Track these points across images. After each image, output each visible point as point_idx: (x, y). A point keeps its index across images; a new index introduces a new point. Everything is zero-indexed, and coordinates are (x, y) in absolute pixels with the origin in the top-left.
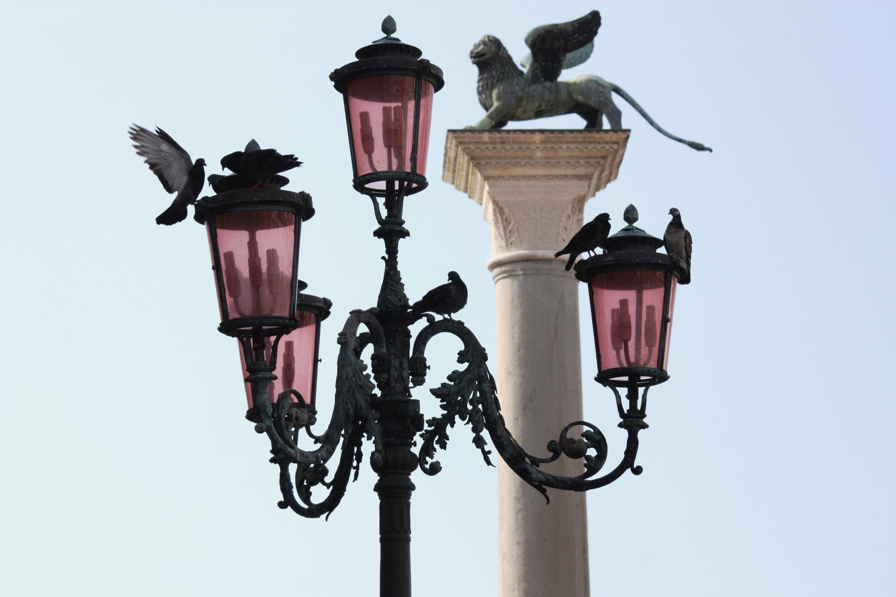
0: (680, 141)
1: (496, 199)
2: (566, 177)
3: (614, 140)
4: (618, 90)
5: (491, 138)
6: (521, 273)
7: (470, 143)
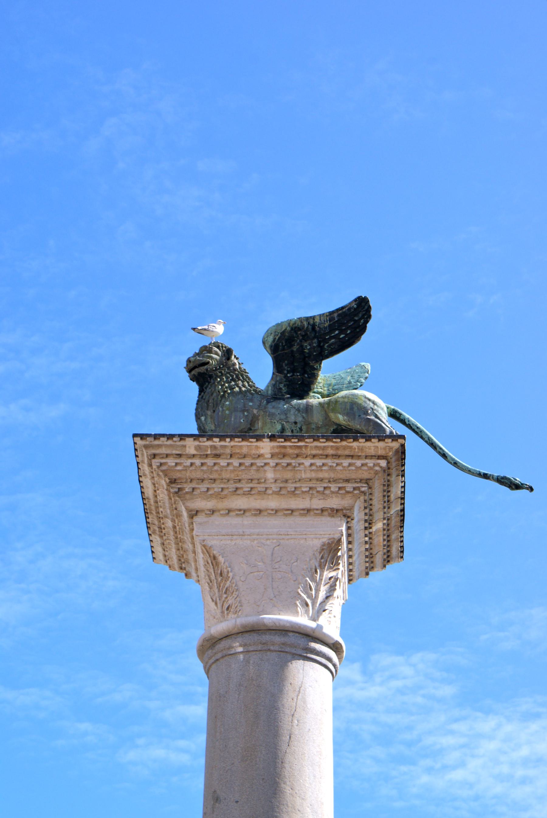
0: (485, 476)
1: (209, 543)
2: (308, 511)
3: (381, 452)
4: (394, 415)
5: (198, 448)
6: (240, 649)
7: (167, 456)
